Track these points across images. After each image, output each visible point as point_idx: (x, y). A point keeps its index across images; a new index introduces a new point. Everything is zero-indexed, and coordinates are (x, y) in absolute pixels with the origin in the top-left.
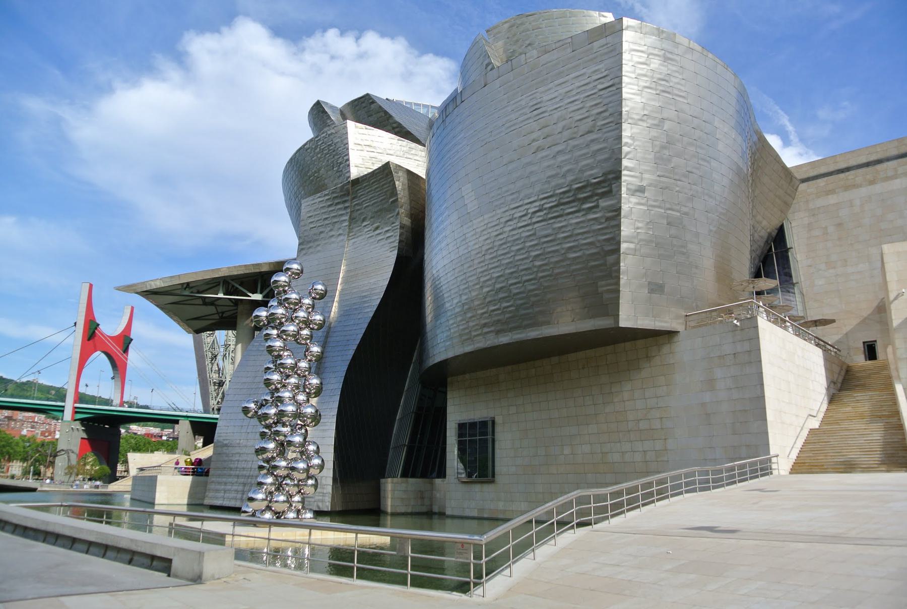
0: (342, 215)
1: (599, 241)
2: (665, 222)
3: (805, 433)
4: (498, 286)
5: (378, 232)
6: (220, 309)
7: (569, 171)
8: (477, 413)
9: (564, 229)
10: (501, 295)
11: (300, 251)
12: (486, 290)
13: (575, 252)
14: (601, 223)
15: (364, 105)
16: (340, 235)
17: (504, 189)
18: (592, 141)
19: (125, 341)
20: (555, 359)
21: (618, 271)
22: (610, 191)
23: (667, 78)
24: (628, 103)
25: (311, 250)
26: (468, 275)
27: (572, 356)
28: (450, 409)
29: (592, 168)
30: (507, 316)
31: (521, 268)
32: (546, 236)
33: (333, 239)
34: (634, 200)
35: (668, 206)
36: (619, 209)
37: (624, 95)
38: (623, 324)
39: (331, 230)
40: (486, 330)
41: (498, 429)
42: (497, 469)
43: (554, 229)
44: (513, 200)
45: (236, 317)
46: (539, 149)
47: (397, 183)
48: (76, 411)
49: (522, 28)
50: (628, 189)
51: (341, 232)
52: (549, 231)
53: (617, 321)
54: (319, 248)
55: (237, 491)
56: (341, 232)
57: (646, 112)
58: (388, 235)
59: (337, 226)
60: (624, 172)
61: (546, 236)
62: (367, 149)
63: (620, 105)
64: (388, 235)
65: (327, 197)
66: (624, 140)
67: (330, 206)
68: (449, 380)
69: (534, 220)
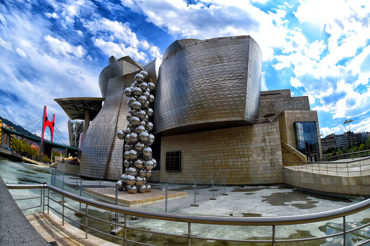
1: (239, 92)
4: (197, 104)
6: (80, 112)
8: (174, 148)
9: (226, 88)
12: (192, 105)
13: (230, 95)
16: (121, 90)
17: (202, 74)
20: (206, 132)
25: (111, 94)
27: (214, 131)
33: (118, 91)
39: (118, 89)
44: (206, 77)
45: (85, 116)
51: (121, 89)
55: (90, 172)
56: (121, 89)
59: (120, 87)
65: (117, 79)
67: (118, 81)
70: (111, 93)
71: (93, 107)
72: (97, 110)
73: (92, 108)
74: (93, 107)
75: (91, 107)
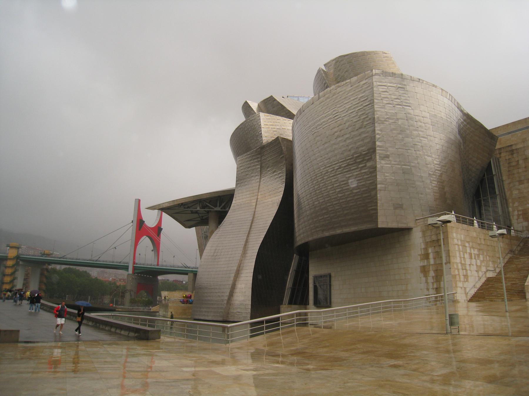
0: (257, 165)
2: (401, 172)
3: (483, 280)
4: (322, 207)
5: (275, 174)
6: (201, 215)
7: (352, 148)
8: (323, 271)
10: (324, 211)
11: (237, 185)
14: (368, 175)
15: (270, 102)
17: (323, 157)
18: (362, 132)
19: (158, 229)
21: (377, 199)
22: (371, 158)
23: (399, 97)
24: (378, 113)
25: (242, 184)
26: (319, 196)
28: (310, 269)
29: (363, 146)
30: (327, 222)
31: (332, 197)
32: (343, 181)
33: (253, 178)
34: (383, 162)
35: (403, 163)
36: (375, 168)
37: (376, 109)
38: (380, 226)
40: (318, 229)
41: (332, 279)
42: (332, 300)
43: (346, 178)
44: (327, 162)
46: (339, 136)
47: (283, 147)
48: (134, 268)
49: (342, 63)
50: (380, 157)
51: (256, 174)
52: (344, 179)
53: (377, 224)
54: (246, 183)
56: (256, 174)
57: (388, 117)
58: (280, 175)
60: (377, 148)
61: (343, 181)
62: (271, 127)
63: (374, 114)
64: (280, 175)
66: (377, 132)
67: (251, 160)
68: (310, 253)
69: (337, 173)
70: (242, 183)
71: (219, 206)
72: (227, 209)
73: (218, 209)
74: (219, 206)
75: (216, 206)
